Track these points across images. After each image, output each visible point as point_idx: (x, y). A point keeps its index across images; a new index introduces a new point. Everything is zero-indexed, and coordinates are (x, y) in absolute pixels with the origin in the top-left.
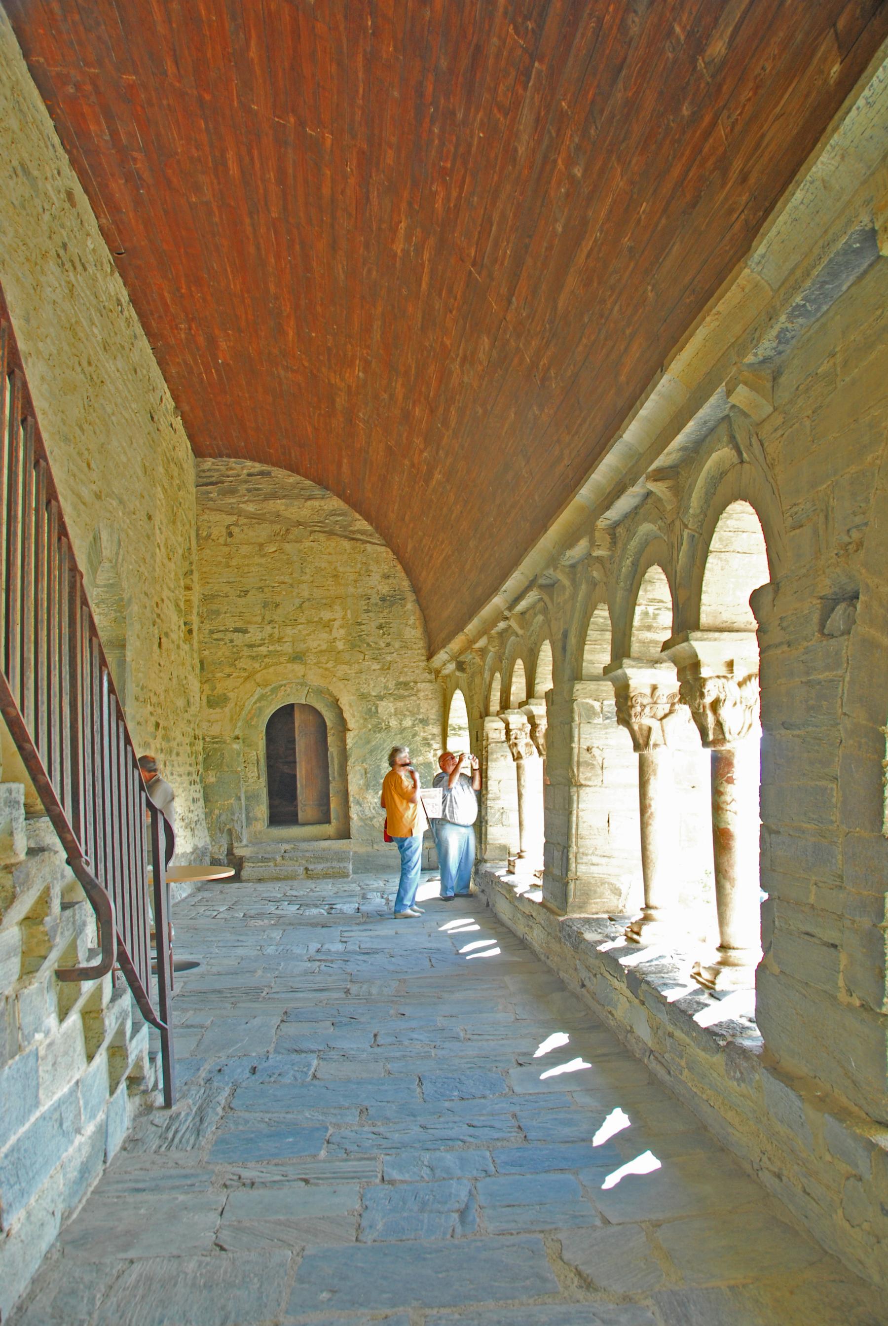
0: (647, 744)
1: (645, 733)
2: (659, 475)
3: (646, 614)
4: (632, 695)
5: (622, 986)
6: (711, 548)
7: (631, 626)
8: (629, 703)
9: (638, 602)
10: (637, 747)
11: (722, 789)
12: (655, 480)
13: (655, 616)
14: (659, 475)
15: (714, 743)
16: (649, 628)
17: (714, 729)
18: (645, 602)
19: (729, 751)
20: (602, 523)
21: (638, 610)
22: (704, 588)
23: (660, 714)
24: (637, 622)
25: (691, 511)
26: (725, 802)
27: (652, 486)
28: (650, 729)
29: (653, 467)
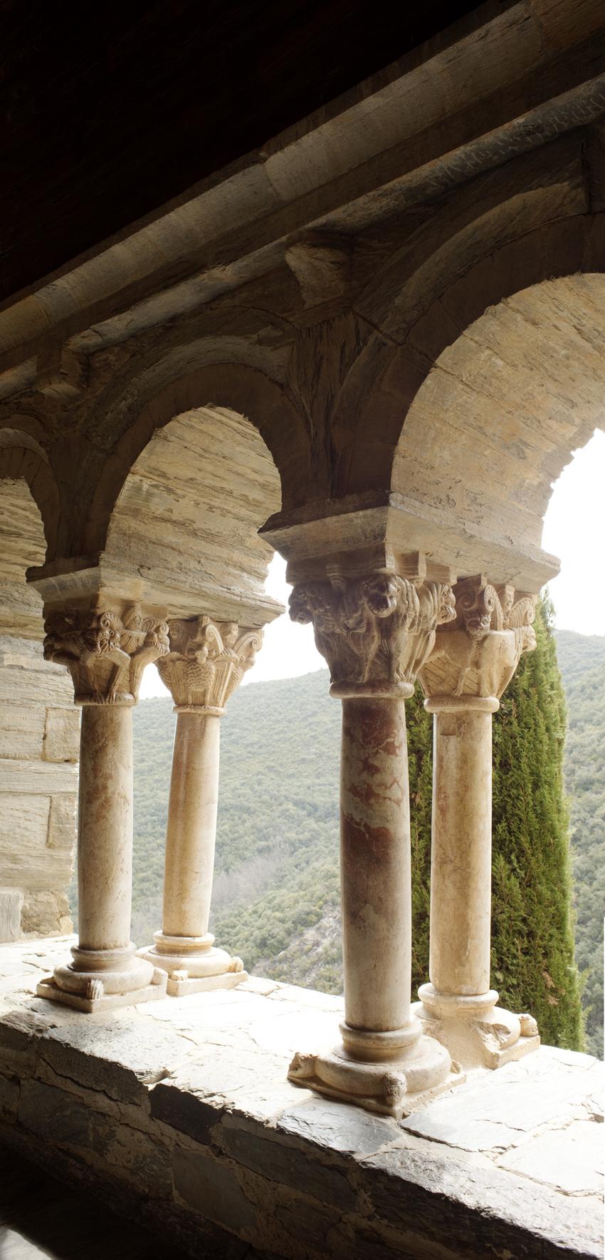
0: (107, 692)
1: (105, 674)
2: (326, 238)
3: (138, 489)
4: (99, 612)
5: (139, 1114)
6: (438, 362)
7: (110, 504)
8: (94, 625)
9: (133, 469)
10: (83, 692)
11: (376, 763)
12: (314, 246)
13: (150, 495)
14: (326, 238)
15: (373, 685)
16: (135, 513)
17: (374, 663)
18: (142, 471)
19: (389, 700)
20: (85, 339)
21: (131, 480)
22: (405, 427)
23: (133, 646)
24: (121, 501)
25: (398, 301)
26: (380, 785)
27: (297, 259)
28: (115, 669)
29: (338, 215)
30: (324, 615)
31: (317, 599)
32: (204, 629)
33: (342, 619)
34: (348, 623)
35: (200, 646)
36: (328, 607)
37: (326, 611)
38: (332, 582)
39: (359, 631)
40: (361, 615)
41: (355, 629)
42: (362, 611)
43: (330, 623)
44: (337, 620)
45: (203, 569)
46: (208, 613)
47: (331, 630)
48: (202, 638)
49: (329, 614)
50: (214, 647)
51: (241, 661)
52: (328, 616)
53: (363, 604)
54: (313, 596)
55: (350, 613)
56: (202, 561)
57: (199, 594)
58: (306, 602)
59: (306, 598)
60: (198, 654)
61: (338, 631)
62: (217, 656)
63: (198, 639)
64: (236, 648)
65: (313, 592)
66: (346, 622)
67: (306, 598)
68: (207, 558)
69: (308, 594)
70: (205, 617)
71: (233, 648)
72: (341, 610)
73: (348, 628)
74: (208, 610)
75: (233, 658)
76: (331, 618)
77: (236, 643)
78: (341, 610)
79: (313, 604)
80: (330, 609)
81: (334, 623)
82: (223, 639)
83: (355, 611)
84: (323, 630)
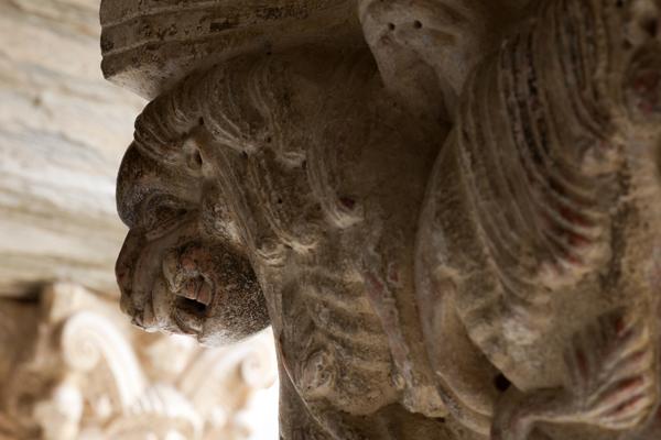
30: (318, 281)
31: (275, 168)
32: (57, 332)
33: (449, 310)
34: (495, 340)
35: (48, 386)
36: (343, 220)
37: (332, 252)
38: (373, 32)
39: (595, 416)
40: (610, 277)
41: (554, 396)
42: (617, 243)
43: (363, 338)
44: (410, 318)
45: (53, 127)
46: (77, 274)
47: (380, 397)
48: (52, 360)
49: (355, 277)
50: (101, 382)
51: (208, 426)
52: (347, 292)
53: (623, 181)
54: (250, 148)
55: (508, 260)
56: (49, 97)
57: (24, 210)
58: (210, 188)
59: (208, 169)
60: (42, 412)
61: (425, 399)
62: (116, 415)
63: (41, 361)
64: (188, 384)
65: (253, 122)
66: (479, 336)
67: (208, 169)
68: (65, 91)
69: (226, 139)
70: (61, 290)
71: (177, 384)
72: (434, 239)
73: (502, 383)
74: (74, 263)
75: (177, 420)
76: (366, 305)
77: (189, 367)
78: (434, 239)
79: (250, 205)
80: (358, 236)
81: (394, 341)
82: (143, 359)
83: (559, 242)
84: (324, 390)
